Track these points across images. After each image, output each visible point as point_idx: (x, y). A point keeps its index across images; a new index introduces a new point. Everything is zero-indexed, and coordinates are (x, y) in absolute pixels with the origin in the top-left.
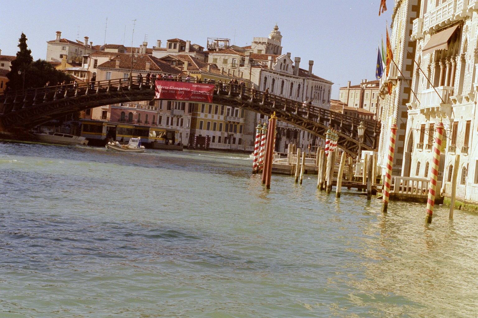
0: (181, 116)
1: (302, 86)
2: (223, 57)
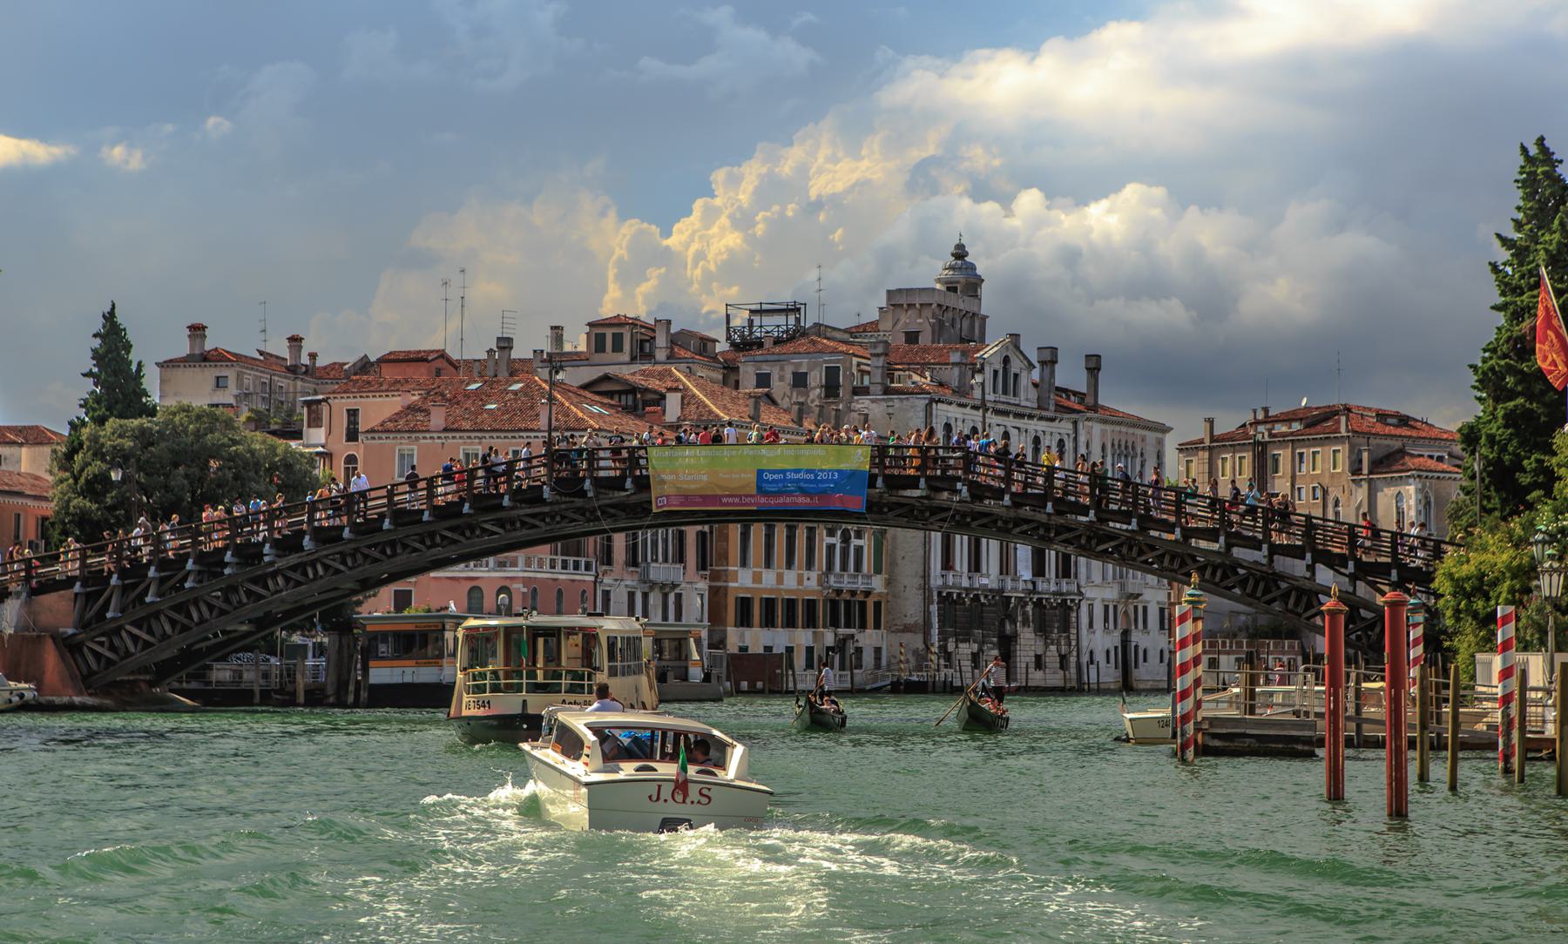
0: (674, 586)
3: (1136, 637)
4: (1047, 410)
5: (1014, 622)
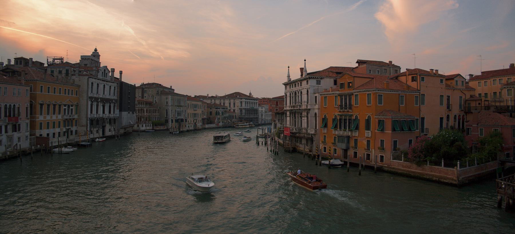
2: (58, 69)
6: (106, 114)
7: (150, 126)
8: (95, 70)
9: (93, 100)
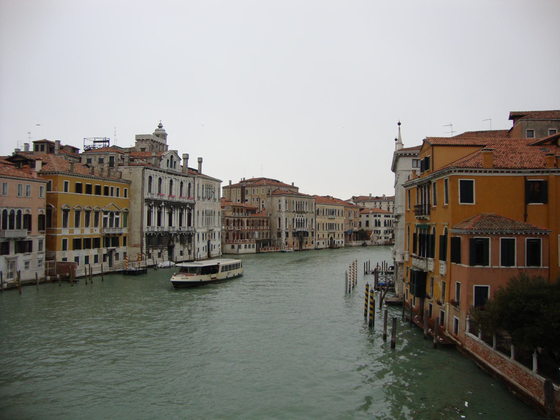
1: (192, 185)
2: (98, 157)
3: (212, 242)
4: (185, 173)
5: (173, 241)
6: (174, 228)
7: (253, 247)
8: (155, 157)
9: (151, 204)
